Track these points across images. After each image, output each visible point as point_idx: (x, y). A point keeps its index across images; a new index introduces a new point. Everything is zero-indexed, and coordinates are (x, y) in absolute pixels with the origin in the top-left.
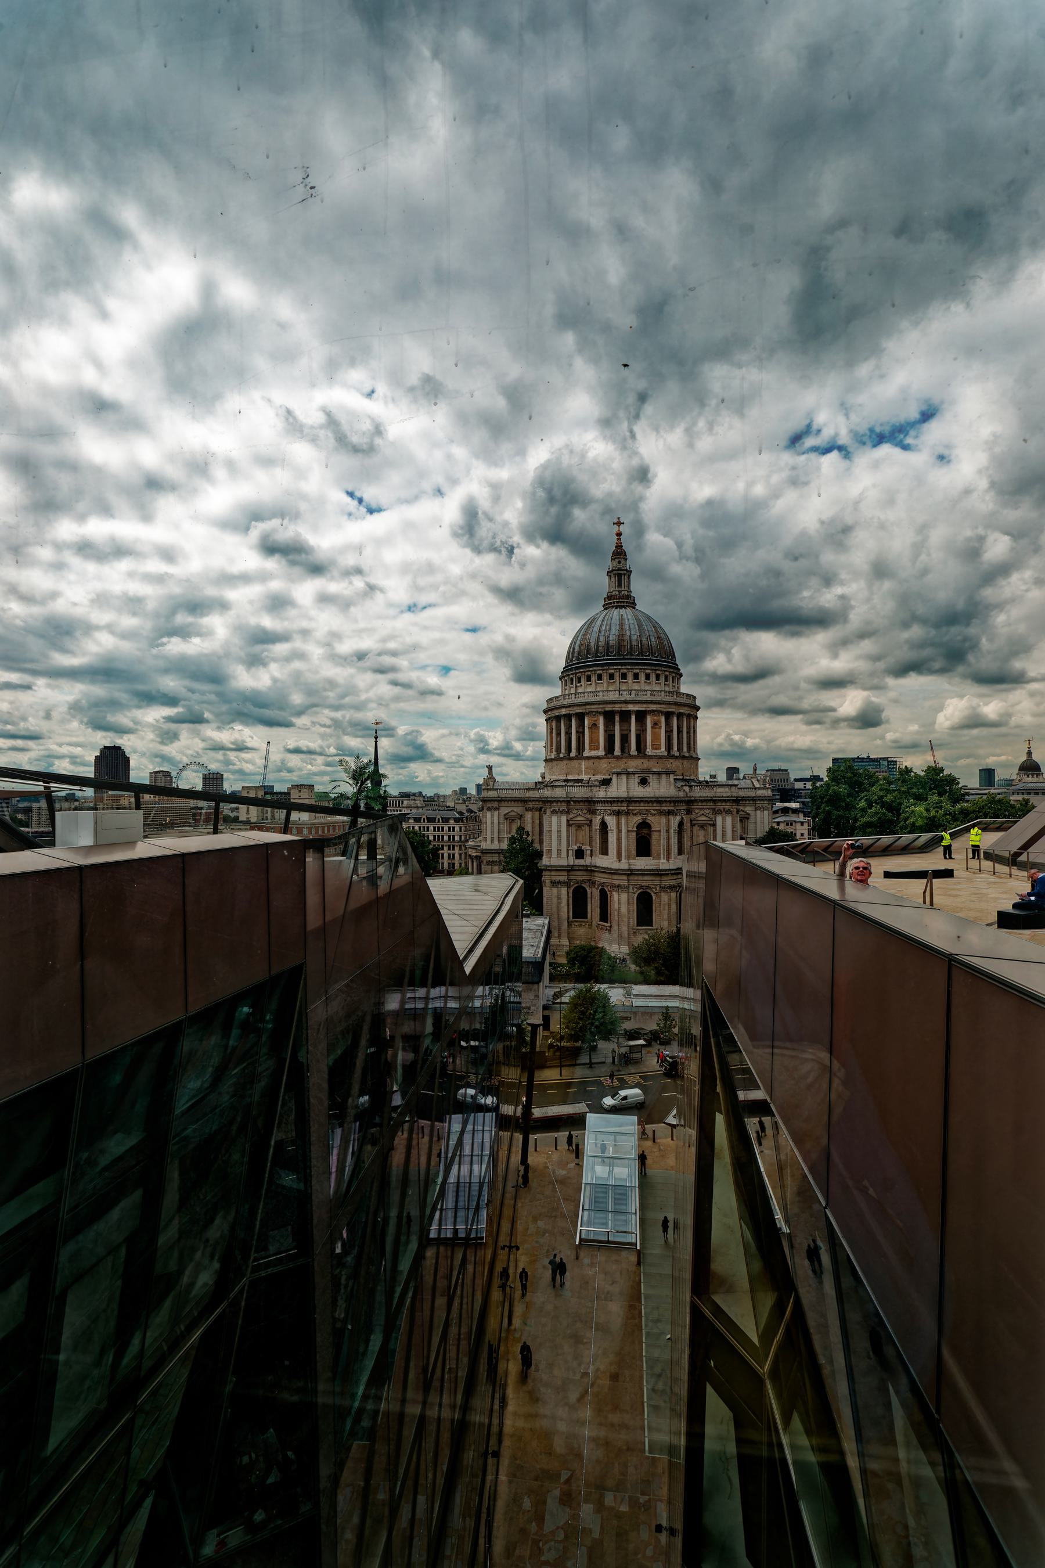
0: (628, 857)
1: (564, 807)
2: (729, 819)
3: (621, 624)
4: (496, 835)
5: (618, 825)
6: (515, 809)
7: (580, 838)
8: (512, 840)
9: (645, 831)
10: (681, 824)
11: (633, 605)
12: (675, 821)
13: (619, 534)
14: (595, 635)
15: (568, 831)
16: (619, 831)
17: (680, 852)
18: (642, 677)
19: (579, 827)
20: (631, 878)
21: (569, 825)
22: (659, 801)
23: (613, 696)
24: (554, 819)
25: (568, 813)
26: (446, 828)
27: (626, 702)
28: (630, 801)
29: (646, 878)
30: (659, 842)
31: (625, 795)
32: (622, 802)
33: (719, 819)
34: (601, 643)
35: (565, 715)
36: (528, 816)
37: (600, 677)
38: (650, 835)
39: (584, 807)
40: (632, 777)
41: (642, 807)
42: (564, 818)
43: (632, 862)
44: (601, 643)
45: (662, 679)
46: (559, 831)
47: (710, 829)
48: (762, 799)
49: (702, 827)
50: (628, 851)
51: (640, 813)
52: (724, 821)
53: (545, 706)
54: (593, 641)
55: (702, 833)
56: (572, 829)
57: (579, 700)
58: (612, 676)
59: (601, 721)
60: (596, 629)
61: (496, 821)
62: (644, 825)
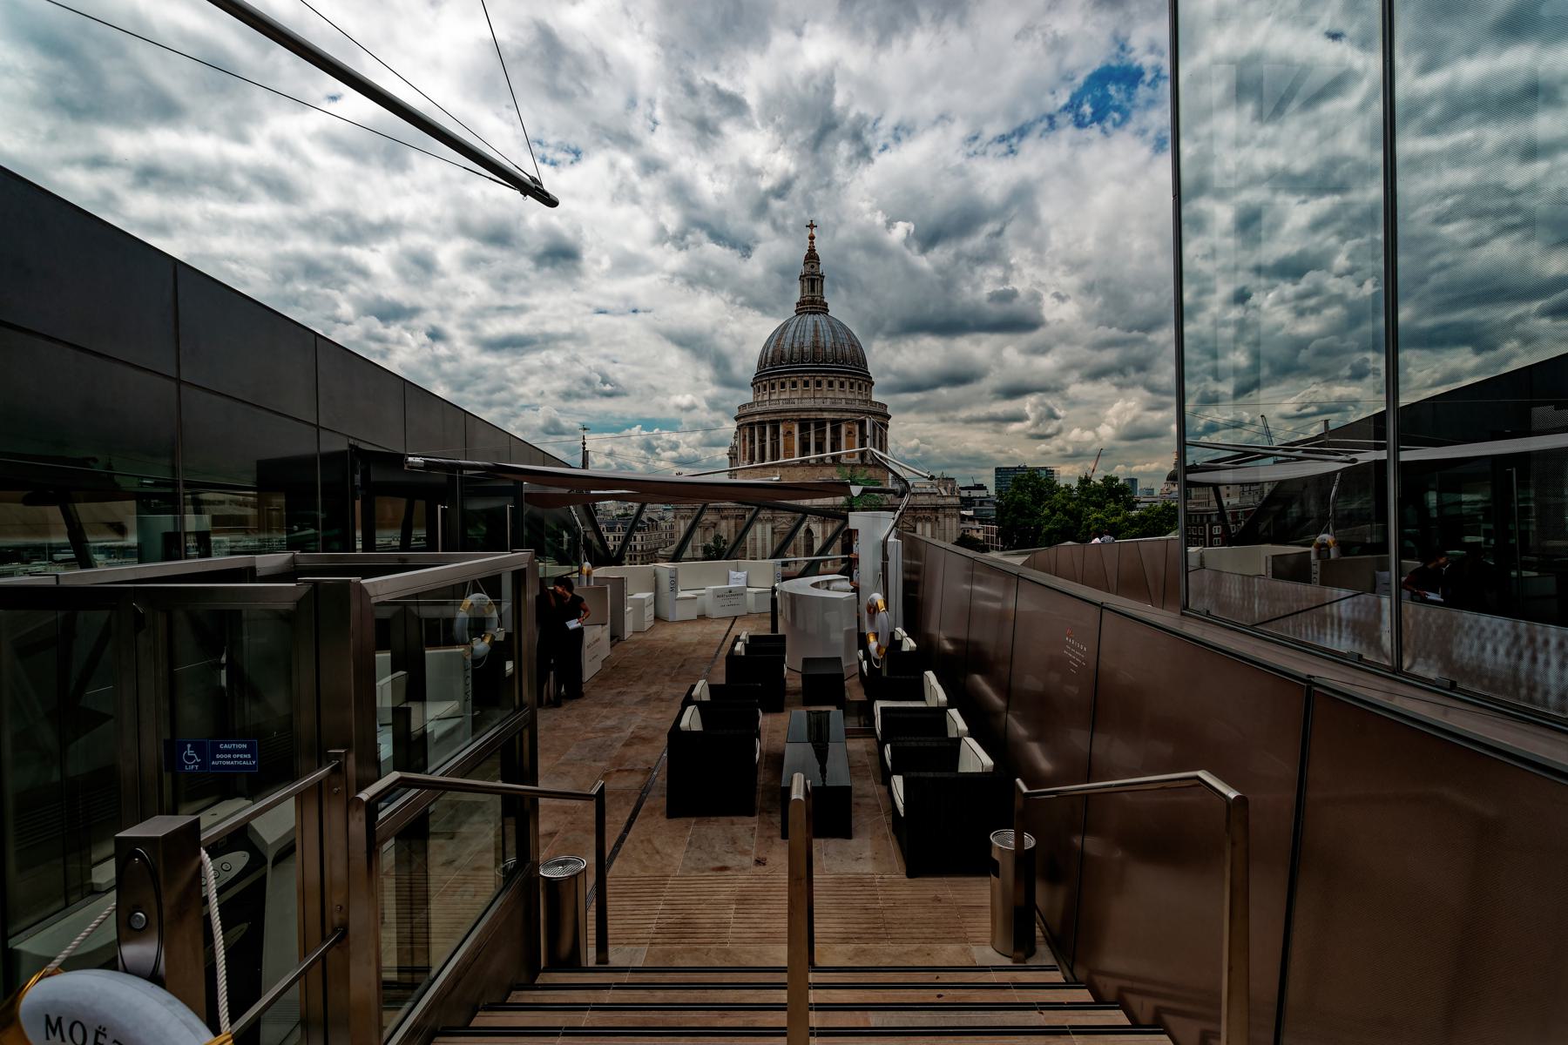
2: (928, 526)
3: (816, 331)
11: (825, 310)
13: (812, 238)
14: (789, 341)
18: (837, 385)
21: (773, 533)
23: (808, 404)
25: (773, 520)
27: (821, 410)
33: (919, 526)
34: (796, 349)
36: (723, 524)
37: (794, 384)
44: (796, 349)
46: (764, 540)
48: (951, 507)
53: (737, 413)
54: (787, 347)
57: (773, 407)
60: (790, 334)
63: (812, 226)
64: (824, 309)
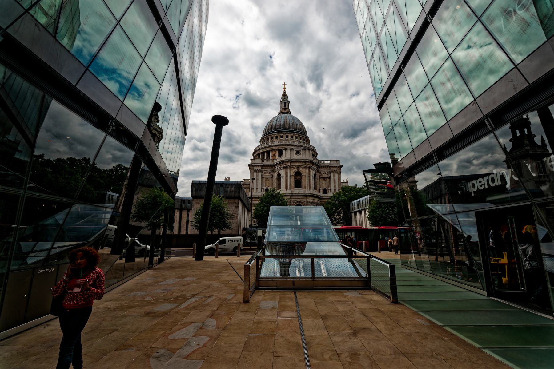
0: (291, 188)
1: (260, 168)
5: (286, 173)
7: (267, 184)
9: (299, 177)
10: (315, 175)
11: (290, 113)
12: (313, 173)
13: (285, 89)
14: (275, 122)
15: (262, 180)
16: (286, 176)
17: (315, 188)
18: (294, 137)
19: (267, 178)
20: (292, 198)
21: (262, 177)
22: (305, 161)
23: (283, 143)
24: (255, 174)
25: (262, 171)
28: (291, 161)
29: (299, 197)
30: (305, 181)
31: (289, 158)
32: (288, 161)
33: (332, 175)
35: (262, 153)
37: (277, 137)
38: (301, 179)
39: (269, 169)
40: (292, 151)
41: (298, 164)
42: (260, 174)
43: (292, 190)
44: (278, 124)
45: (302, 140)
47: (328, 180)
49: (325, 179)
50: (291, 185)
51: (296, 167)
52: (334, 176)
54: (274, 124)
55: (324, 182)
56: (264, 180)
58: (282, 137)
59: (277, 153)
60: (275, 120)
62: (298, 174)
63: (285, 85)
64: (290, 113)
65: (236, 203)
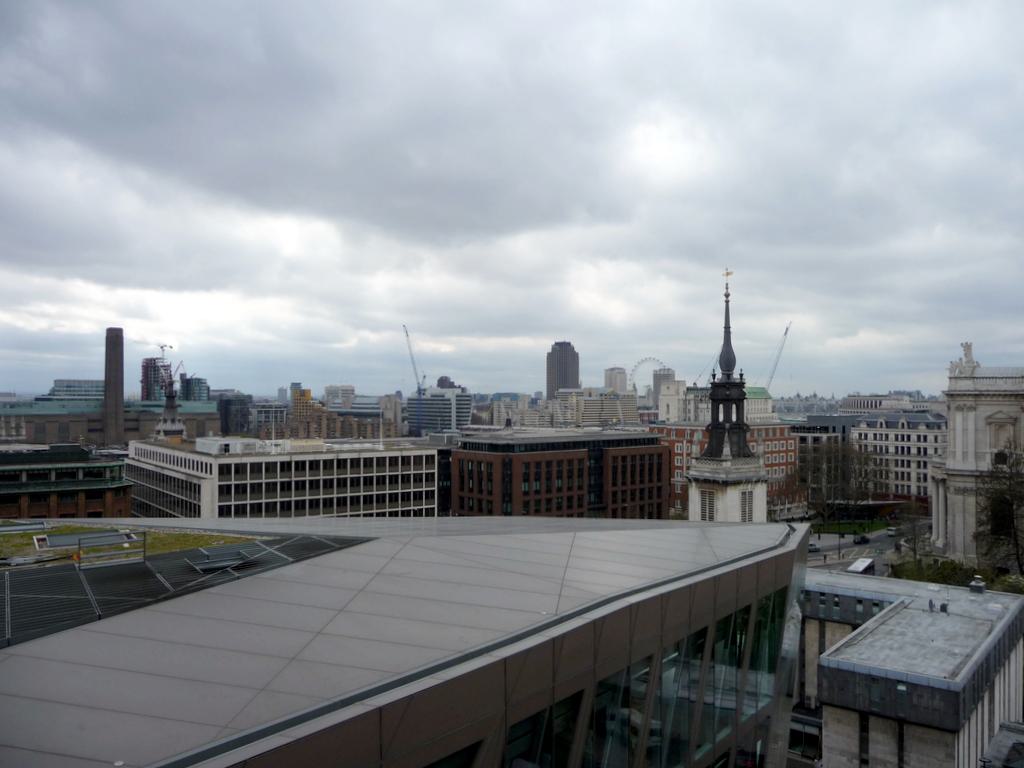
4: (971, 449)
6: (1005, 409)
8: (1000, 458)
26: (914, 437)
61: (971, 426)
65: (947, 745)
